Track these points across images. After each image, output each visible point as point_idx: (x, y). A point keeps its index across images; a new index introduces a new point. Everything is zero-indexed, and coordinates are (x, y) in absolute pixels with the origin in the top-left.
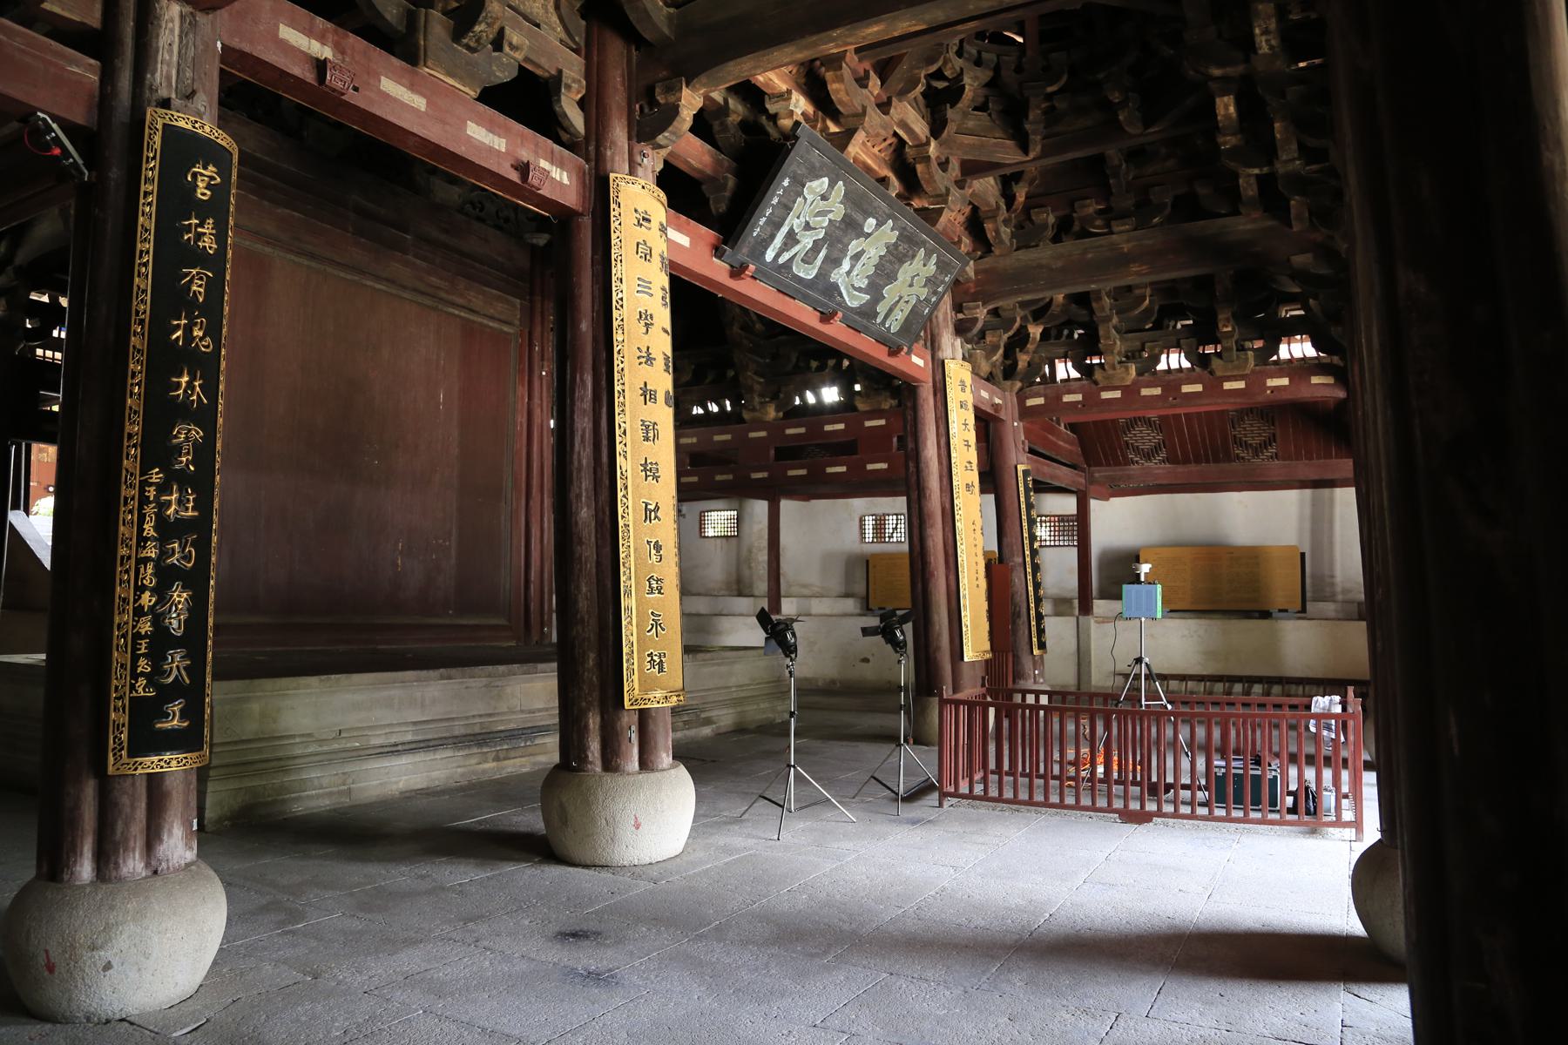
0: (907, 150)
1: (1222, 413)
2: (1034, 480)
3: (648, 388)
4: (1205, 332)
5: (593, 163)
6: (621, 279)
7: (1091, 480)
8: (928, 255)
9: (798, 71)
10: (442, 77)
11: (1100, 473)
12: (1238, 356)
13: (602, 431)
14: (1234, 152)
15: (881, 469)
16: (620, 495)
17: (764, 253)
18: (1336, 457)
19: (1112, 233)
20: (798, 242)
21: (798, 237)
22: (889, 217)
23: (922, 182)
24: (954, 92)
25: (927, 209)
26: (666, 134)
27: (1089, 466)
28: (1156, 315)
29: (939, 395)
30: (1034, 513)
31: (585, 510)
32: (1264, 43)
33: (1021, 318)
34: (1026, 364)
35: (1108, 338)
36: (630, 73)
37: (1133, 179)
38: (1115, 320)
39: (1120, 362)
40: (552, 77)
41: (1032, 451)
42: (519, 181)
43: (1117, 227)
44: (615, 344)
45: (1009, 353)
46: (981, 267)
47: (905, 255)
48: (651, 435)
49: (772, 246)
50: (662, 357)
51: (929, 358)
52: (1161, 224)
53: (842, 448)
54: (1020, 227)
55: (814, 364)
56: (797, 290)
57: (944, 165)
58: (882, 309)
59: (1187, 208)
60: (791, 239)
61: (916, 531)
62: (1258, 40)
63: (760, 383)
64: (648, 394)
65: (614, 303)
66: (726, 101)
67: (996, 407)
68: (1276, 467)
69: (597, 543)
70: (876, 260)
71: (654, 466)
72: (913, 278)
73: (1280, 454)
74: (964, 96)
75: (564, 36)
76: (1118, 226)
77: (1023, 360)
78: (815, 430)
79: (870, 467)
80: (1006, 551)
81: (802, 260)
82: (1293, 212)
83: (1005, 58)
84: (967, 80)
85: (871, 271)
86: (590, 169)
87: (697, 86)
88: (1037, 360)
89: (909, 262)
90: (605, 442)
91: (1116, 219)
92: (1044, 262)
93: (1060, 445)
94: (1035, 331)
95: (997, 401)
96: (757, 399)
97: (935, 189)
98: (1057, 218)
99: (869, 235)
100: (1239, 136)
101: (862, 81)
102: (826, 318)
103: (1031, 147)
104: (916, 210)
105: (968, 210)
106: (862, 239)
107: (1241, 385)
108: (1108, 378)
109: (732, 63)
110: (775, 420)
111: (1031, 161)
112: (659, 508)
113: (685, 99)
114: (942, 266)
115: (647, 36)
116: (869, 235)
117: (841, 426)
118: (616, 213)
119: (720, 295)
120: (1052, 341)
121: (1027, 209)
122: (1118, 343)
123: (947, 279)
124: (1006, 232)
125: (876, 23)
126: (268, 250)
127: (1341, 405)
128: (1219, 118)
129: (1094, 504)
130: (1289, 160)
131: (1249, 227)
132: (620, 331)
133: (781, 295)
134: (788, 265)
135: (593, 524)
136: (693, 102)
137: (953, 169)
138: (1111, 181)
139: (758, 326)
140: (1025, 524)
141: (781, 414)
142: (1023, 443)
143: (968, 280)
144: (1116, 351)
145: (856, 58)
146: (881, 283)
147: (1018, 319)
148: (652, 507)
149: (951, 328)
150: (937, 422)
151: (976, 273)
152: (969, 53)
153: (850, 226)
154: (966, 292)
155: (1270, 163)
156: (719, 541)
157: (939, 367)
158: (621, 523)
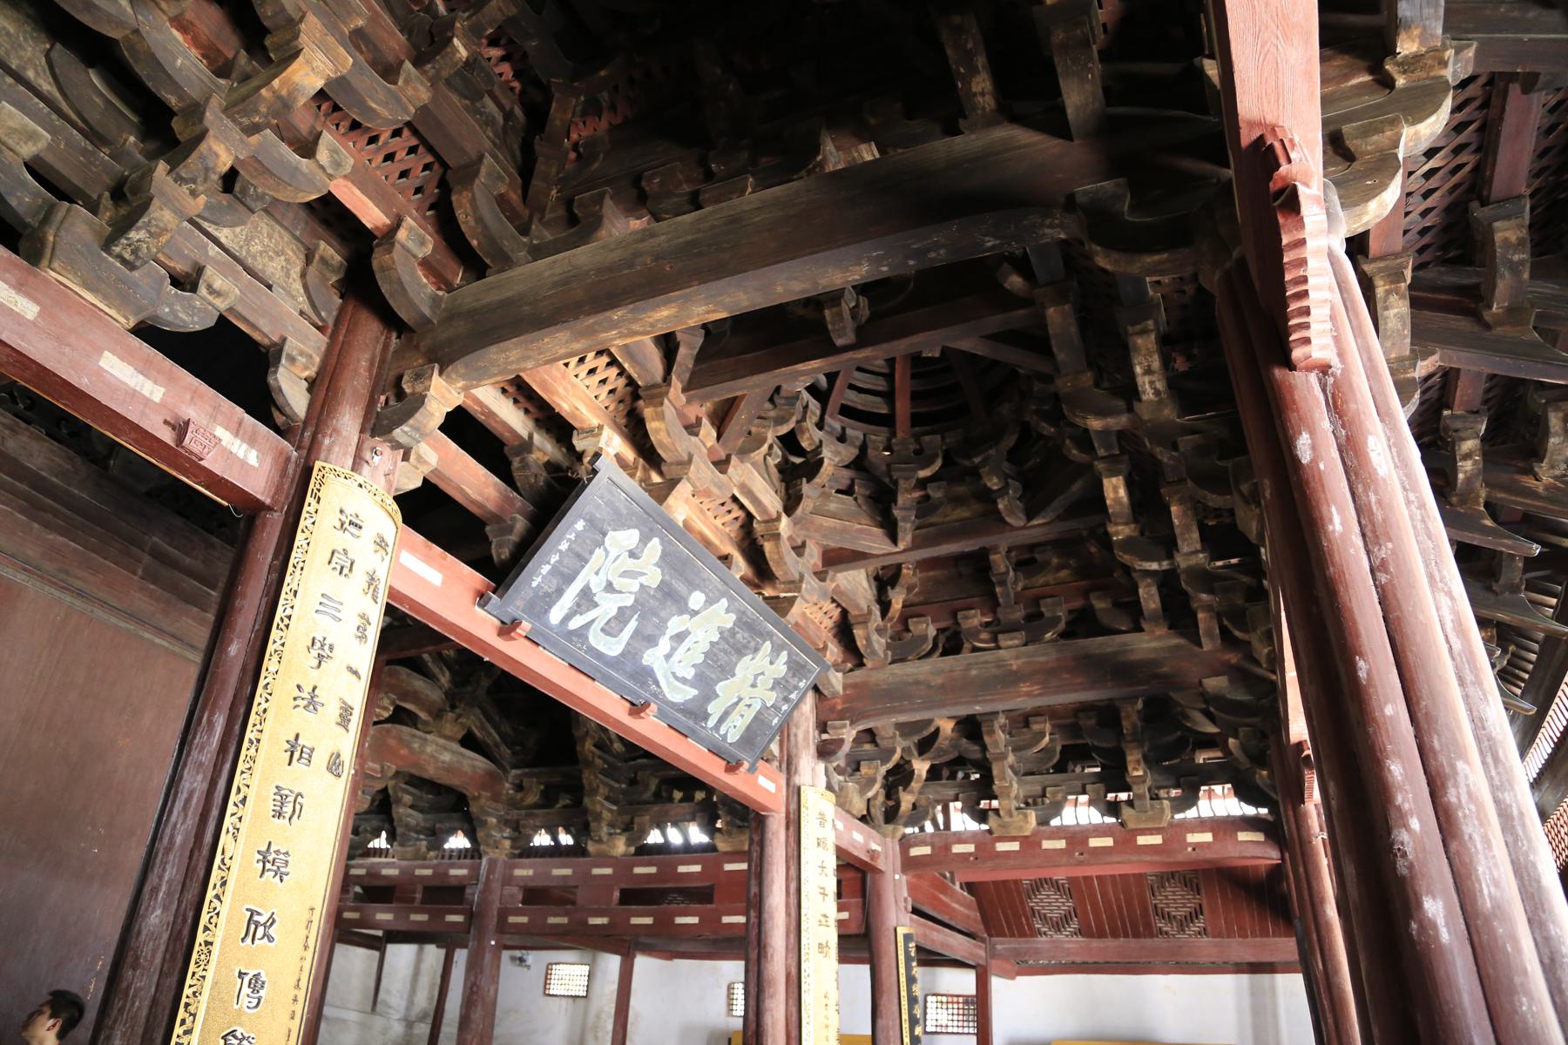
0: (755, 525)
1: (1140, 877)
2: (919, 949)
3: (300, 741)
4: (1115, 777)
5: (304, 452)
6: (296, 592)
7: (993, 954)
8: (777, 650)
9: (616, 409)
10: (76, 289)
11: (1002, 944)
12: (1152, 805)
13: (216, 794)
14: (1128, 544)
15: (738, 924)
16: (210, 894)
17: (547, 611)
18: (1274, 936)
19: (998, 648)
20: (596, 605)
21: (596, 599)
22: (723, 595)
23: (771, 564)
24: (812, 467)
25: (777, 597)
26: (405, 428)
27: (990, 935)
28: (1057, 757)
29: (791, 829)
30: (917, 990)
31: (158, 912)
32: (1147, 386)
33: (903, 750)
34: (911, 806)
35: (1003, 778)
36: (383, 361)
37: (1024, 589)
38: (1011, 758)
39: (1018, 809)
40: (274, 344)
41: (915, 911)
42: (172, 444)
43: (1004, 640)
44: (263, 673)
45: (891, 790)
46: (850, 681)
47: (745, 647)
48: (288, 809)
49: (559, 604)
50: (338, 704)
51: (784, 783)
52: (1052, 641)
53: (699, 895)
54: (896, 637)
55: (678, 795)
56: (597, 669)
57: (799, 549)
58: (715, 709)
59: (1083, 624)
60: (586, 599)
61: (752, 1002)
62: (1140, 380)
63: (611, 811)
64: (296, 751)
65: (277, 620)
66: (531, 436)
67: (873, 854)
68: (1206, 946)
69: (163, 965)
70: (707, 647)
71: (282, 856)
72: (756, 676)
73: (1209, 929)
74: (822, 470)
75: (307, 308)
77: (907, 800)
78: (668, 871)
79: (726, 920)
80: (880, 1036)
81: (603, 630)
82: (1201, 626)
83: (873, 437)
84: (826, 453)
85: (700, 659)
86: (299, 457)
87: (454, 376)
88: (923, 802)
89: (750, 656)
90: (215, 812)
91: (1003, 632)
92: (922, 677)
93: (953, 909)
94: (921, 767)
95: (875, 847)
96: (605, 830)
97: (786, 573)
98: (940, 631)
99: (695, 613)
100: (1133, 526)
101: (692, 428)
102: (637, 709)
103: (900, 535)
104: (765, 599)
105: (836, 613)
106: (687, 617)
107: (1157, 840)
108: (1003, 826)
109: (493, 349)
110: (624, 855)
111: (902, 550)
112: (274, 921)
113: (435, 388)
114: (796, 668)
115: (403, 315)
116: (695, 613)
117: (697, 868)
118: (312, 509)
119: (486, 659)
120: (944, 781)
121: (904, 620)
122: (1015, 785)
123: (802, 685)
124: (879, 643)
125: (666, 303)
126: (20, 578)
127: (1276, 872)
128: (1108, 502)
129: (997, 984)
130: (1190, 551)
131: (1154, 644)
132: (275, 658)
133: (574, 672)
134: (582, 633)
135: (165, 936)
136: (448, 396)
137: (811, 556)
138: (998, 590)
139: (617, 746)
140: (904, 1003)
141: (632, 850)
142: (906, 900)
143: (835, 696)
144: (1013, 795)
145: (683, 398)
146: (713, 676)
147: (899, 750)
148: (262, 919)
149: (812, 749)
150: (787, 861)
151: (845, 688)
152: (830, 426)
153: (669, 597)
154: (832, 709)
155: (1170, 557)
156: (564, 1001)
157: (795, 793)
158: (201, 937)
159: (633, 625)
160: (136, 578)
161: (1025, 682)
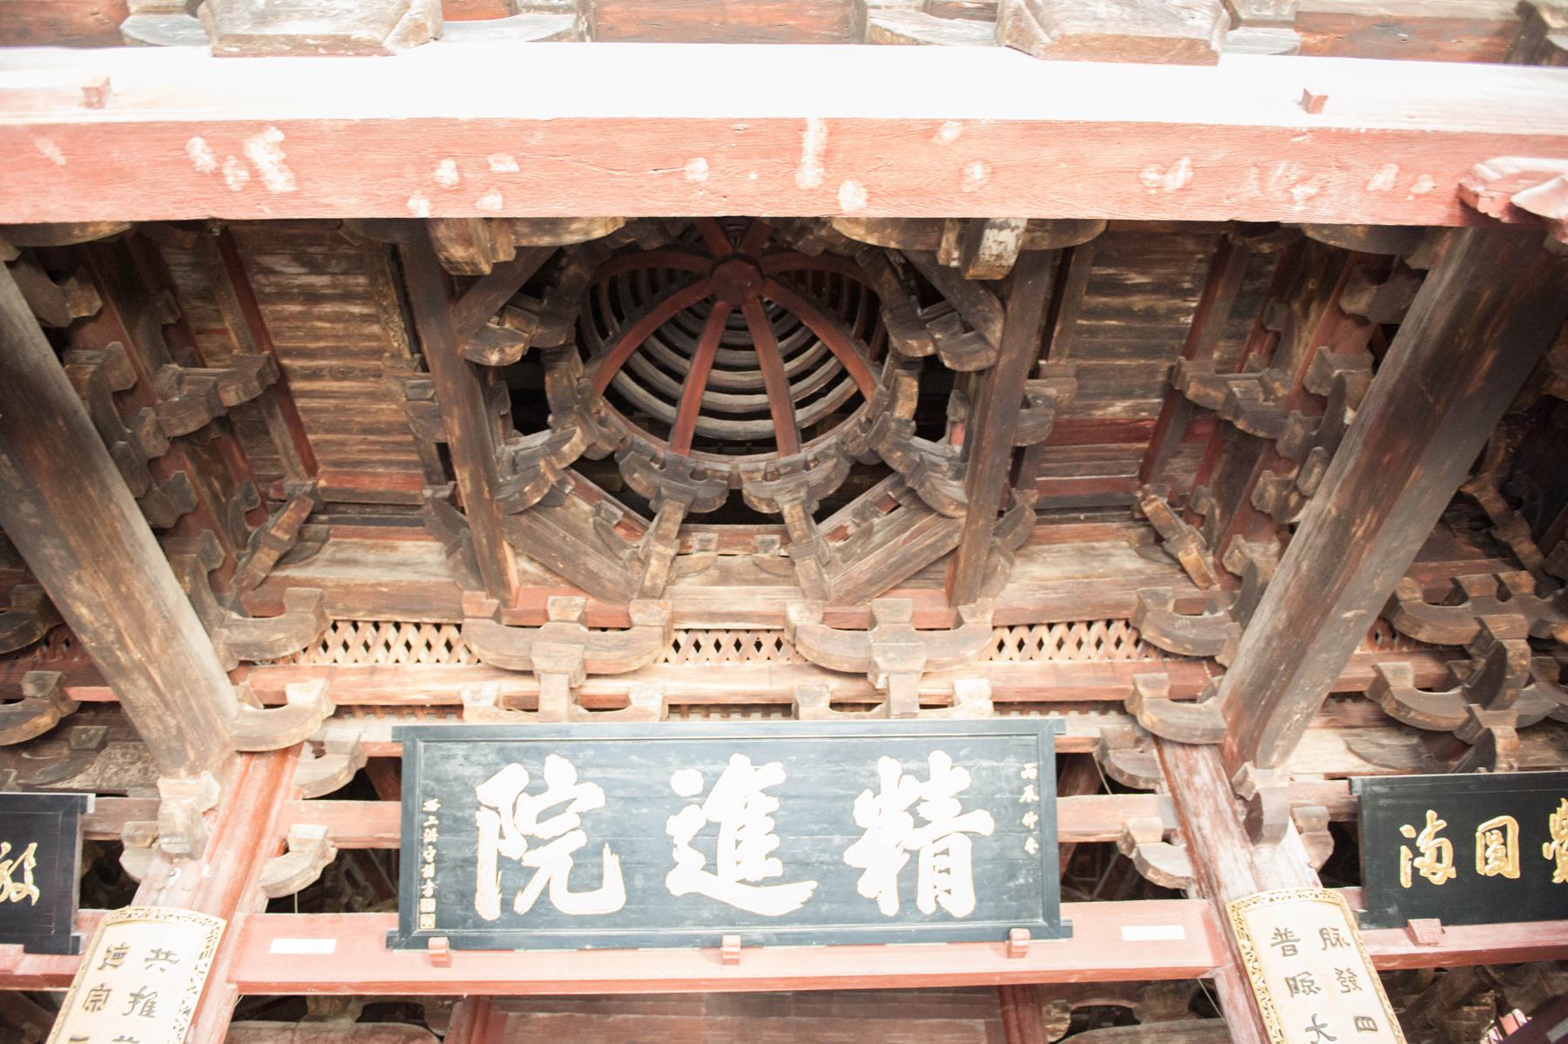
20: (531, 872)
58: (880, 887)
60: (514, 873)
76: (1306, 482)
89: (868, 793)
92: (1268, 630)
138: (1240, 425)
159: (611, 862)
160: (701, 1018)
161: (1353, 523)
